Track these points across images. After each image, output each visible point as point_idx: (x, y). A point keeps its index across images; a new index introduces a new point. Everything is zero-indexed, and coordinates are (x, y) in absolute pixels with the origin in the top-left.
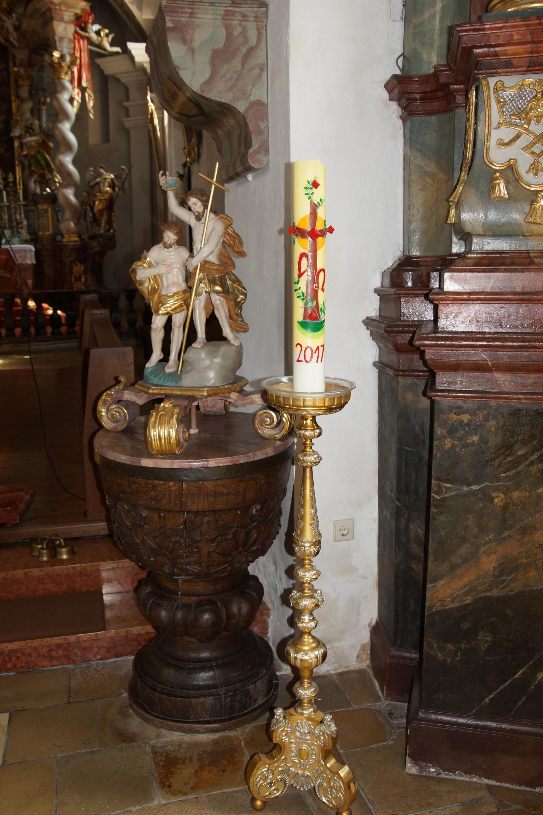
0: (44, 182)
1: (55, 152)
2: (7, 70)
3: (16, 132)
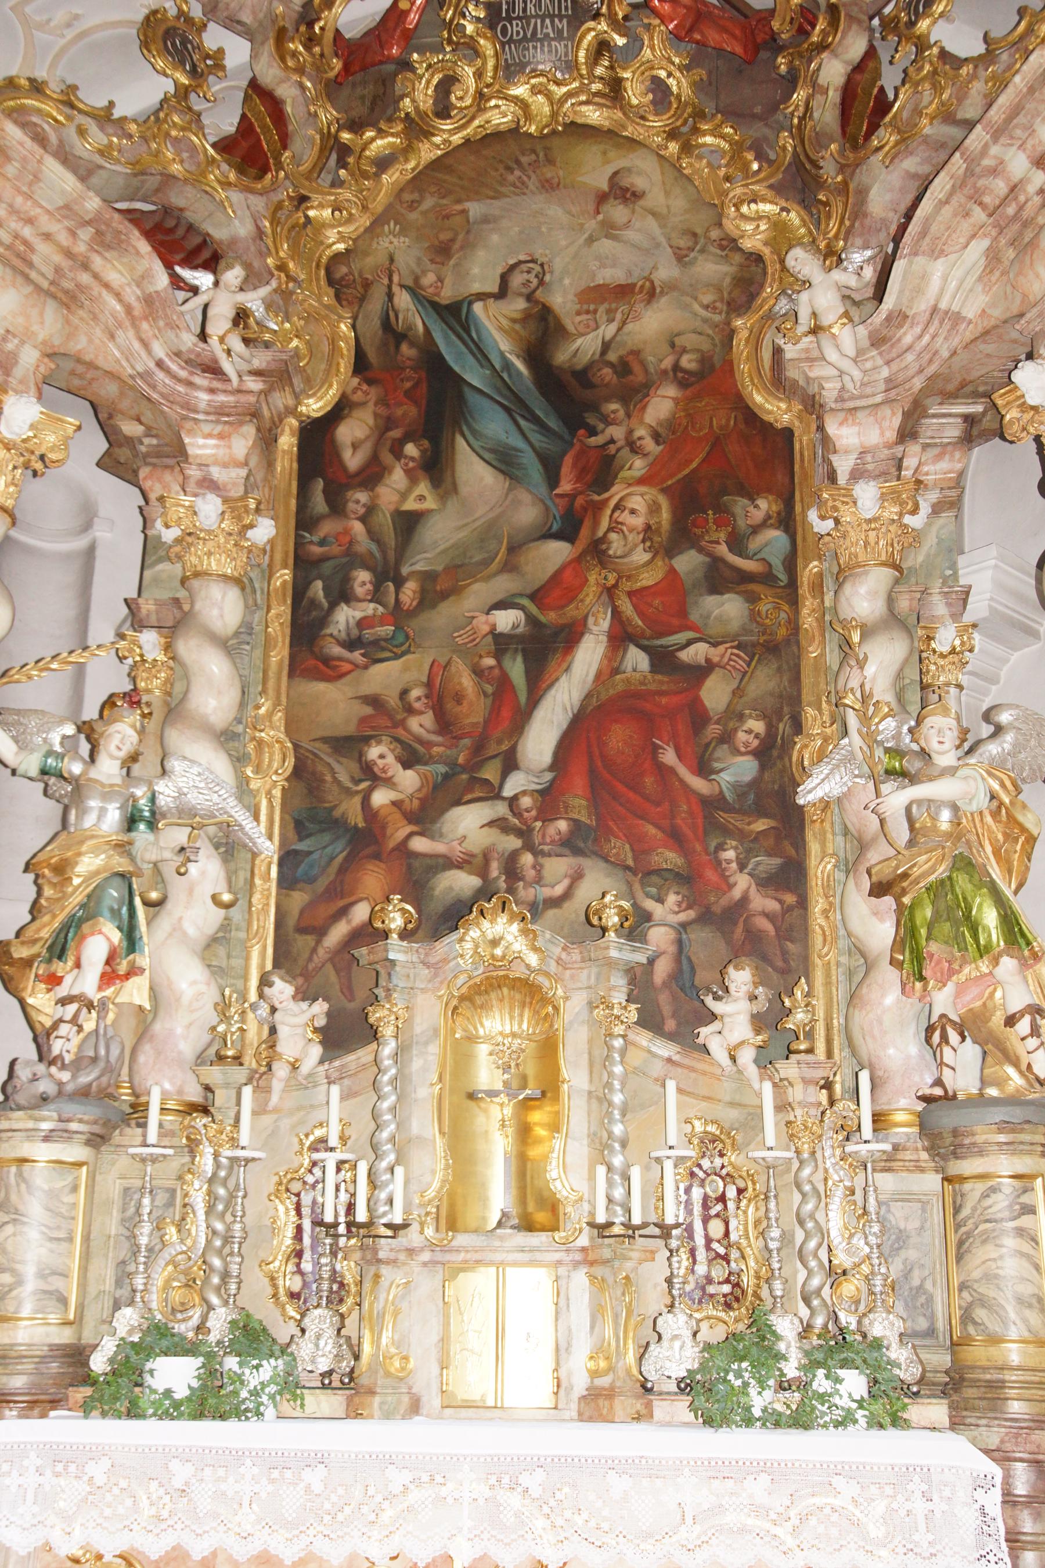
2: (787, 520)
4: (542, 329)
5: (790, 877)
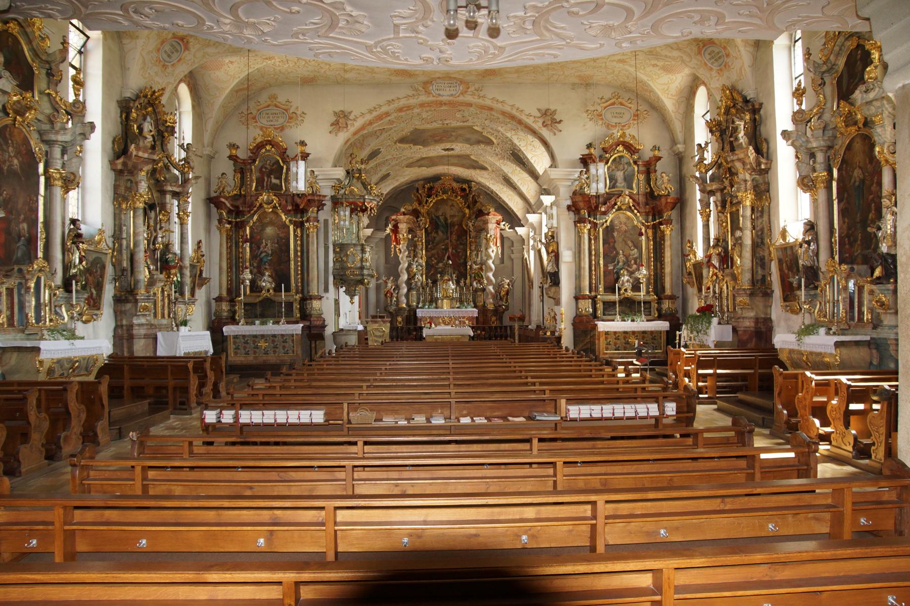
0: (480, 282)
1: (487, 271)
3: (469, 263)
4: (446, 219)
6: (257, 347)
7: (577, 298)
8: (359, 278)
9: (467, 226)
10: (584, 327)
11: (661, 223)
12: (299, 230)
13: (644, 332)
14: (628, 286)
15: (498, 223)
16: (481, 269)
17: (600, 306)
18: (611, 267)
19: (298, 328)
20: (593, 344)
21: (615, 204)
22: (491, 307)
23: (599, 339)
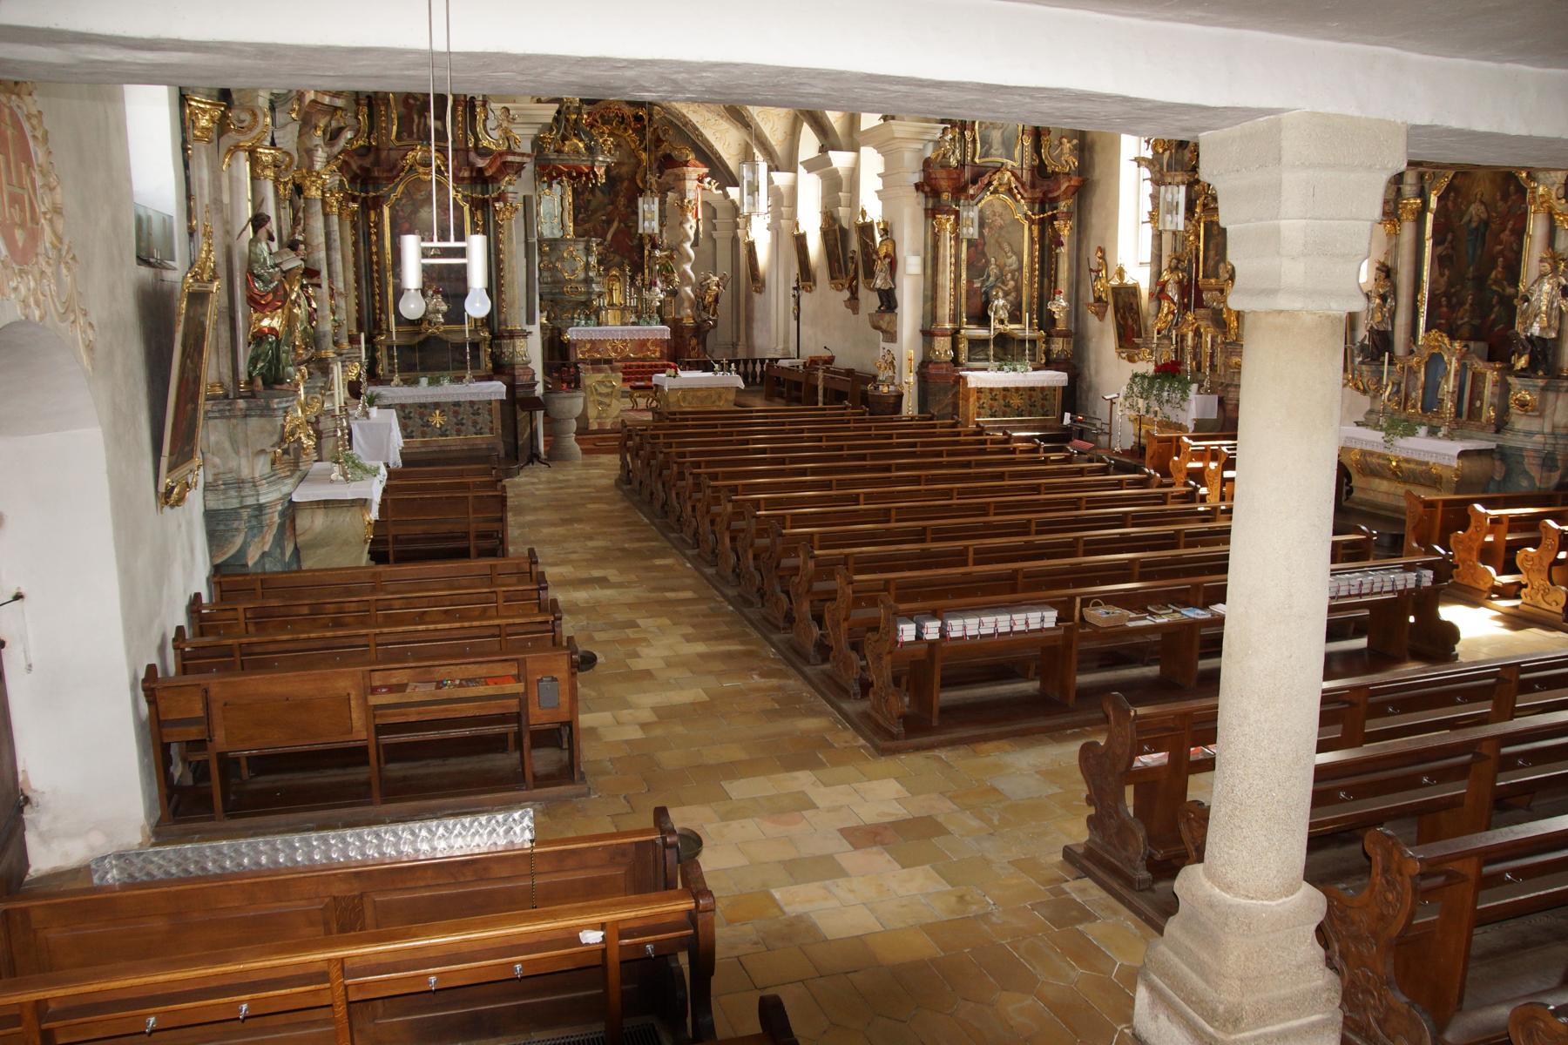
5: (642, 257)
6: (427, 424)
7: (928, 334)
8: (583, 298)
9: (644, 181)
10: (938, 381)
11: (1054, 217)
12: (479, 213)
13: (1032, 389)
14: (1004, 314)
15: (700, 180)
16: (671, 257)
17: (964, 346)
18: (978, 285)
19: (496, 389)
20: (956, 406)
21: (990, 184)
22: (689, 322)
23: (967, 400)
